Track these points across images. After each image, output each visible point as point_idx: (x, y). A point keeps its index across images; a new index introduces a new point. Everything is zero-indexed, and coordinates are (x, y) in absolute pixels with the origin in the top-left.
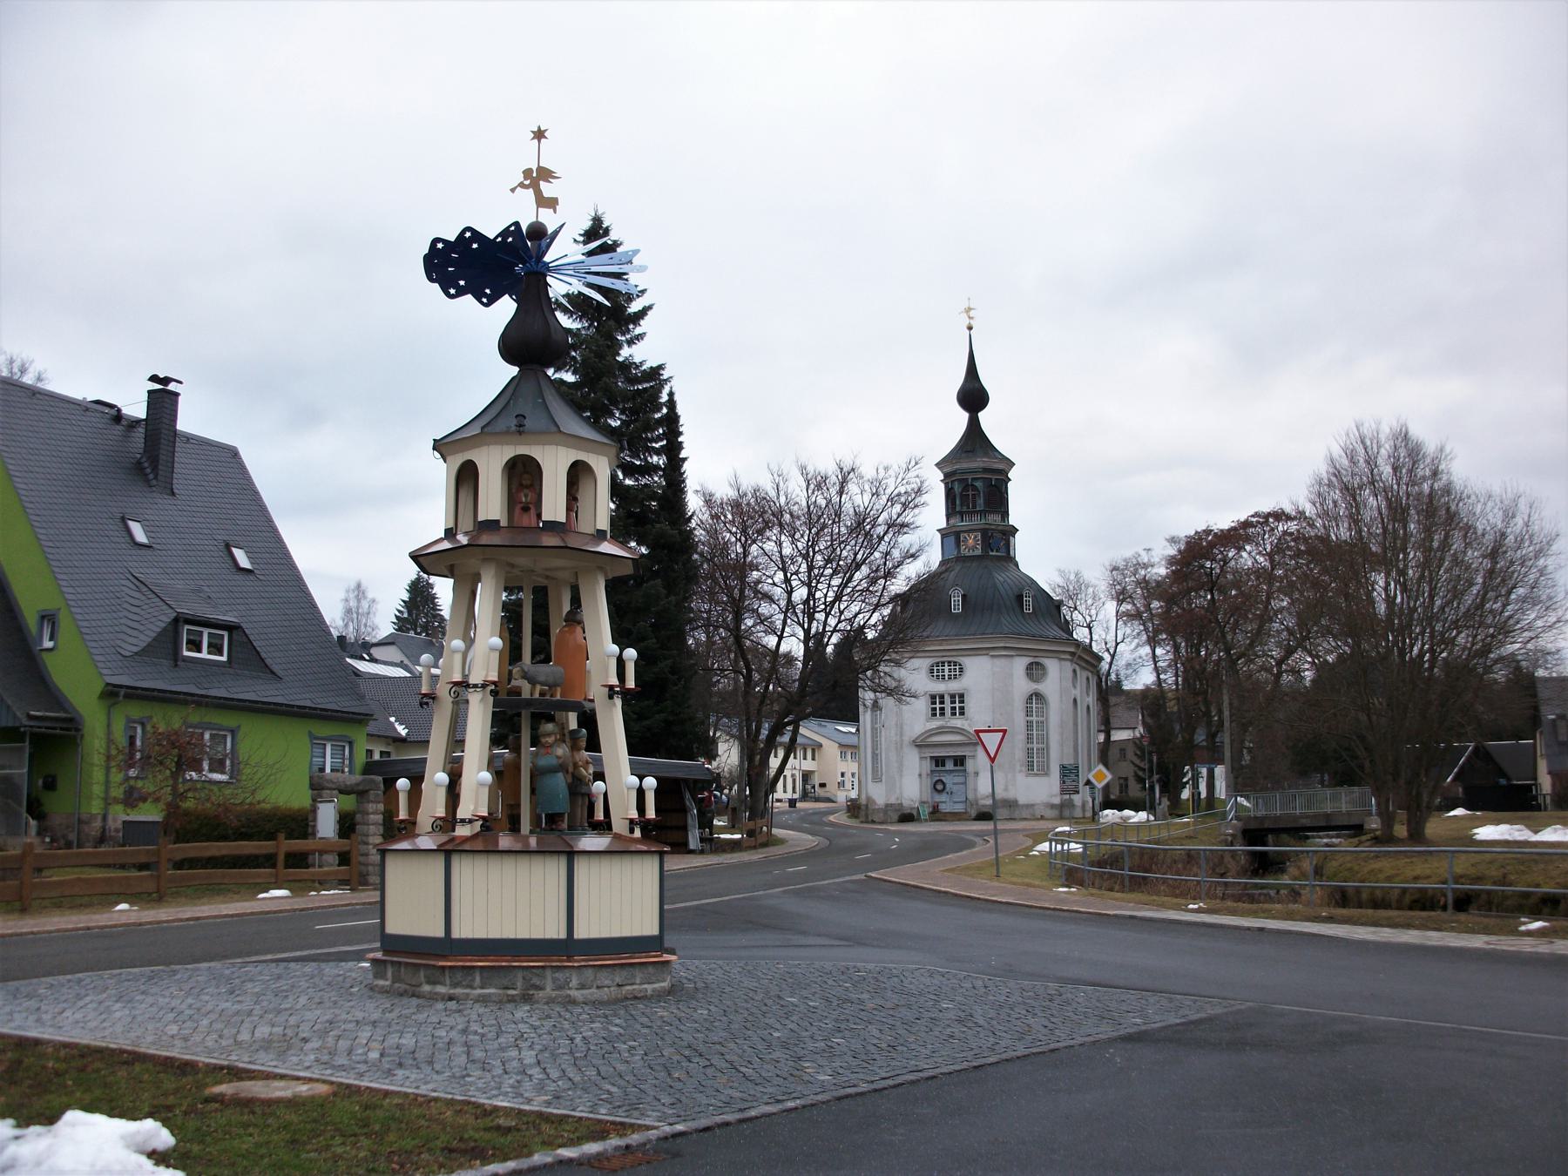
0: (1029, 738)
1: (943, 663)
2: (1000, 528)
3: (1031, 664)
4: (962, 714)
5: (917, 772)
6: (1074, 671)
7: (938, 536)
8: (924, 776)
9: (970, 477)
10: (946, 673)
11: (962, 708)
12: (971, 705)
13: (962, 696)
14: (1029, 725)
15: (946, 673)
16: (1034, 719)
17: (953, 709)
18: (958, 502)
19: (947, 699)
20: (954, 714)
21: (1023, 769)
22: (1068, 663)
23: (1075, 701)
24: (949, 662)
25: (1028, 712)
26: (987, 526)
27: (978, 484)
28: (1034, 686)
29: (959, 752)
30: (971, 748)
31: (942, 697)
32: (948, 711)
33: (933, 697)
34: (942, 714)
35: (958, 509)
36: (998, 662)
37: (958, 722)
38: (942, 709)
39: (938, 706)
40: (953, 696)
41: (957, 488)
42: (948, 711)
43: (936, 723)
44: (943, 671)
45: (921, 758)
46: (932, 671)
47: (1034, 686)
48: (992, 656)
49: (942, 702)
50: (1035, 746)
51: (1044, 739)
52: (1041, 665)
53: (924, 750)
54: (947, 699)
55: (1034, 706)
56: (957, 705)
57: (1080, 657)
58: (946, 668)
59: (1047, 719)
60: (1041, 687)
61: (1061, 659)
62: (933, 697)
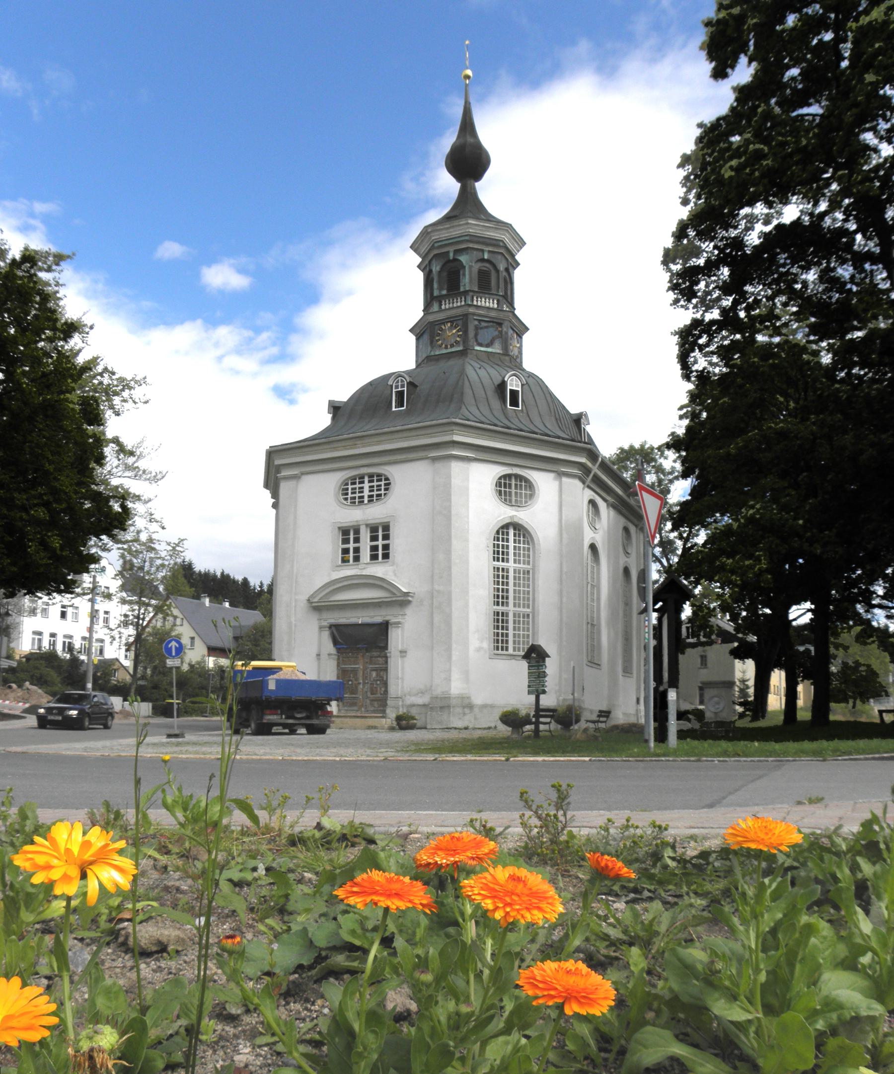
0: (500, 598)
1: (362, 477)
2: (493, 314)
3: (505, 477)
4: (386, 556)
5: (315, 651)
6: (592, 502)
7: (412, 338)
8: (324, 656)
9: (451, 249)
10: (366, 493)
11: (386, 547)
12: (398, 543)
13: (386, 528)
14: (500, 576)
15: (366, 493)
16: (511, 565)
17: (374, 549)
18: (435, 286)
19: (365, 535)
20: (374, 557)
21: (485, 645)
22: (577, 483)
23: (593, 547)
24: (371, 476)
25: (499, 554)
26: (471, 310)
27: (463, 259)
28: (505, 513)
29: (375, 617)
30: (396, 610)
31: (357, 531)
32: (365, 554)
33: (345, 532)
34: (357, 559)
35: (436, 293)
36: (439, 465)
37: (379, 570)
38: (357, 550)
39: (351, 546)
40: (374, 529)
41: (436, 268)
42: (365, 554)
43: (349, 571)
44: (361, 490)
45: (321, 628)
46: (345, 492)
47: (506, 513)
48: (434, 459)
49: (357, 540)
50: (511, 609)
51: (527, 598)
52: (527, 480)
53: (325, 615)
54: (365, 535)
55: (511, 544)
56: (380, 543)
57: (597, 480)
58: (366, 485)
59: (534, 566)
60: (522, 516)
61: (560, 474)
62: (345, 532)
